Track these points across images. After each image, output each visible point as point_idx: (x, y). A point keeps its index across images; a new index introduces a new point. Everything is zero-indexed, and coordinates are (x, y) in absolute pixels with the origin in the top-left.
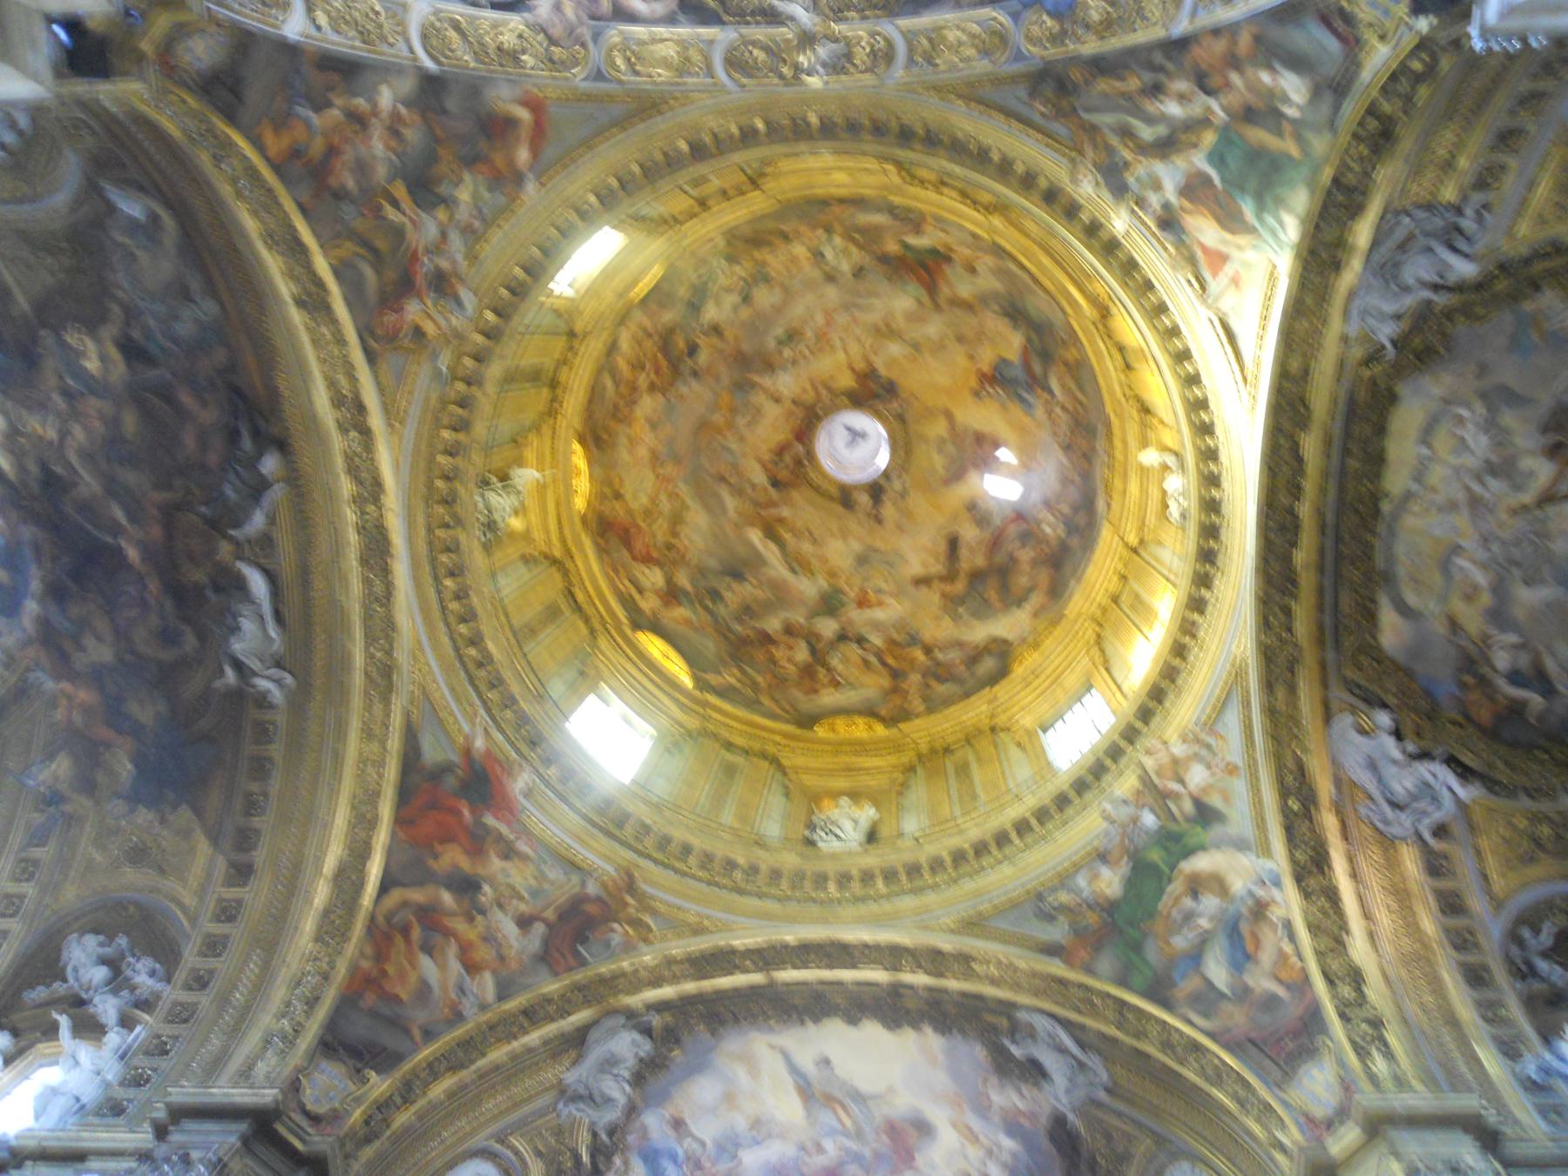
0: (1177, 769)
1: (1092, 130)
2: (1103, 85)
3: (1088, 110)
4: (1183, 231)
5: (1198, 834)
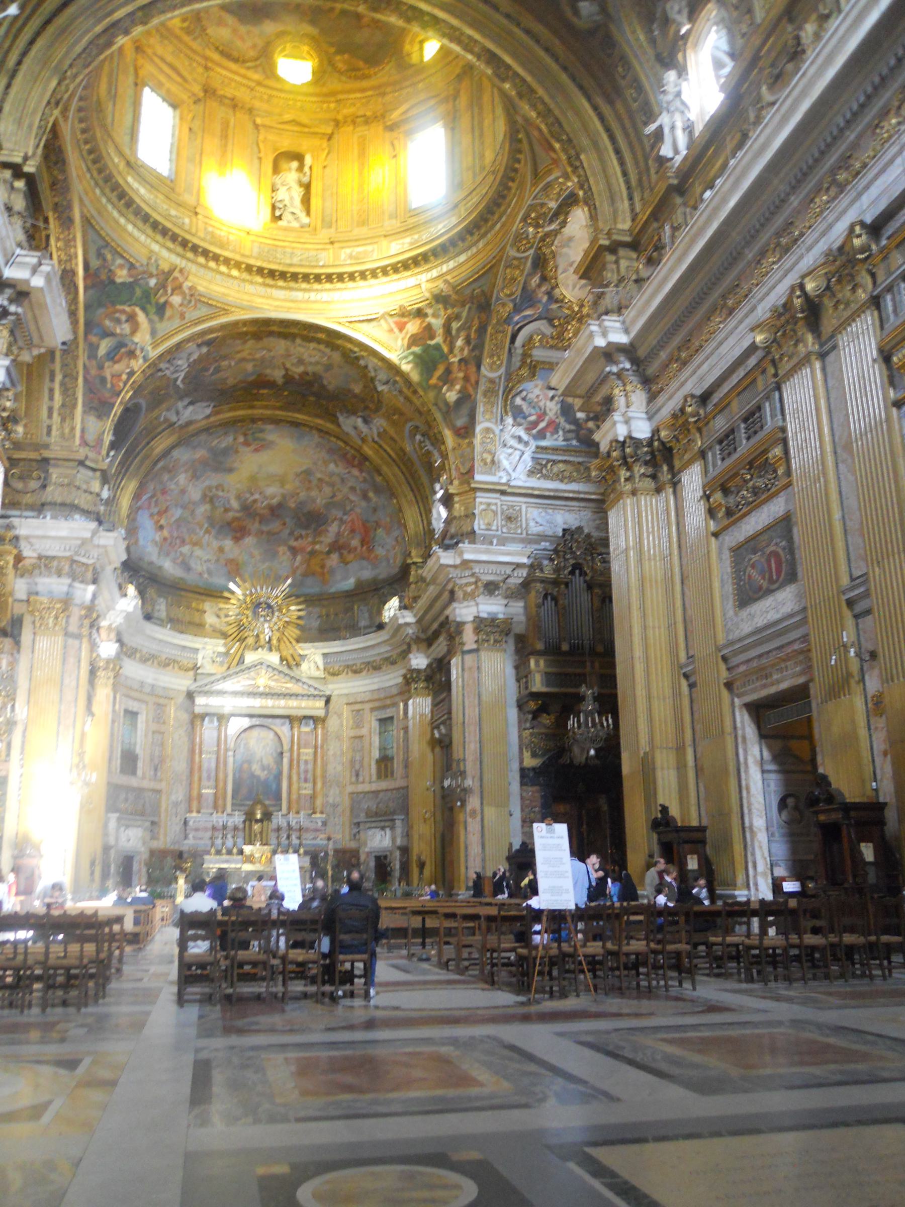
0: (178, 288)
1: (463, 305)
2: (476, 323)
3: (470, 308)
4: (414, 317)
5: (152, 310)
